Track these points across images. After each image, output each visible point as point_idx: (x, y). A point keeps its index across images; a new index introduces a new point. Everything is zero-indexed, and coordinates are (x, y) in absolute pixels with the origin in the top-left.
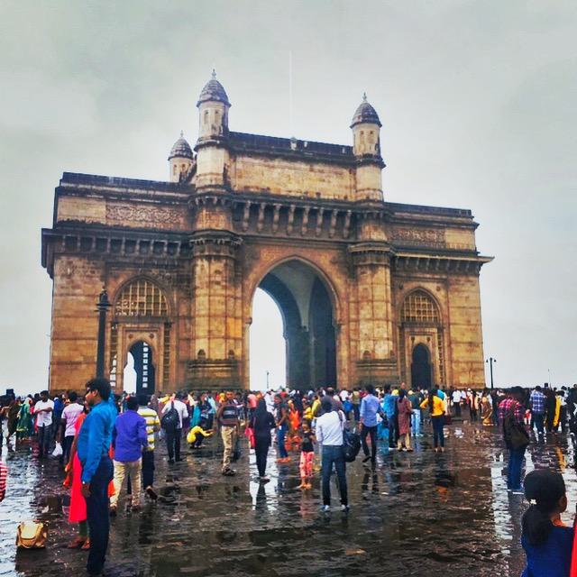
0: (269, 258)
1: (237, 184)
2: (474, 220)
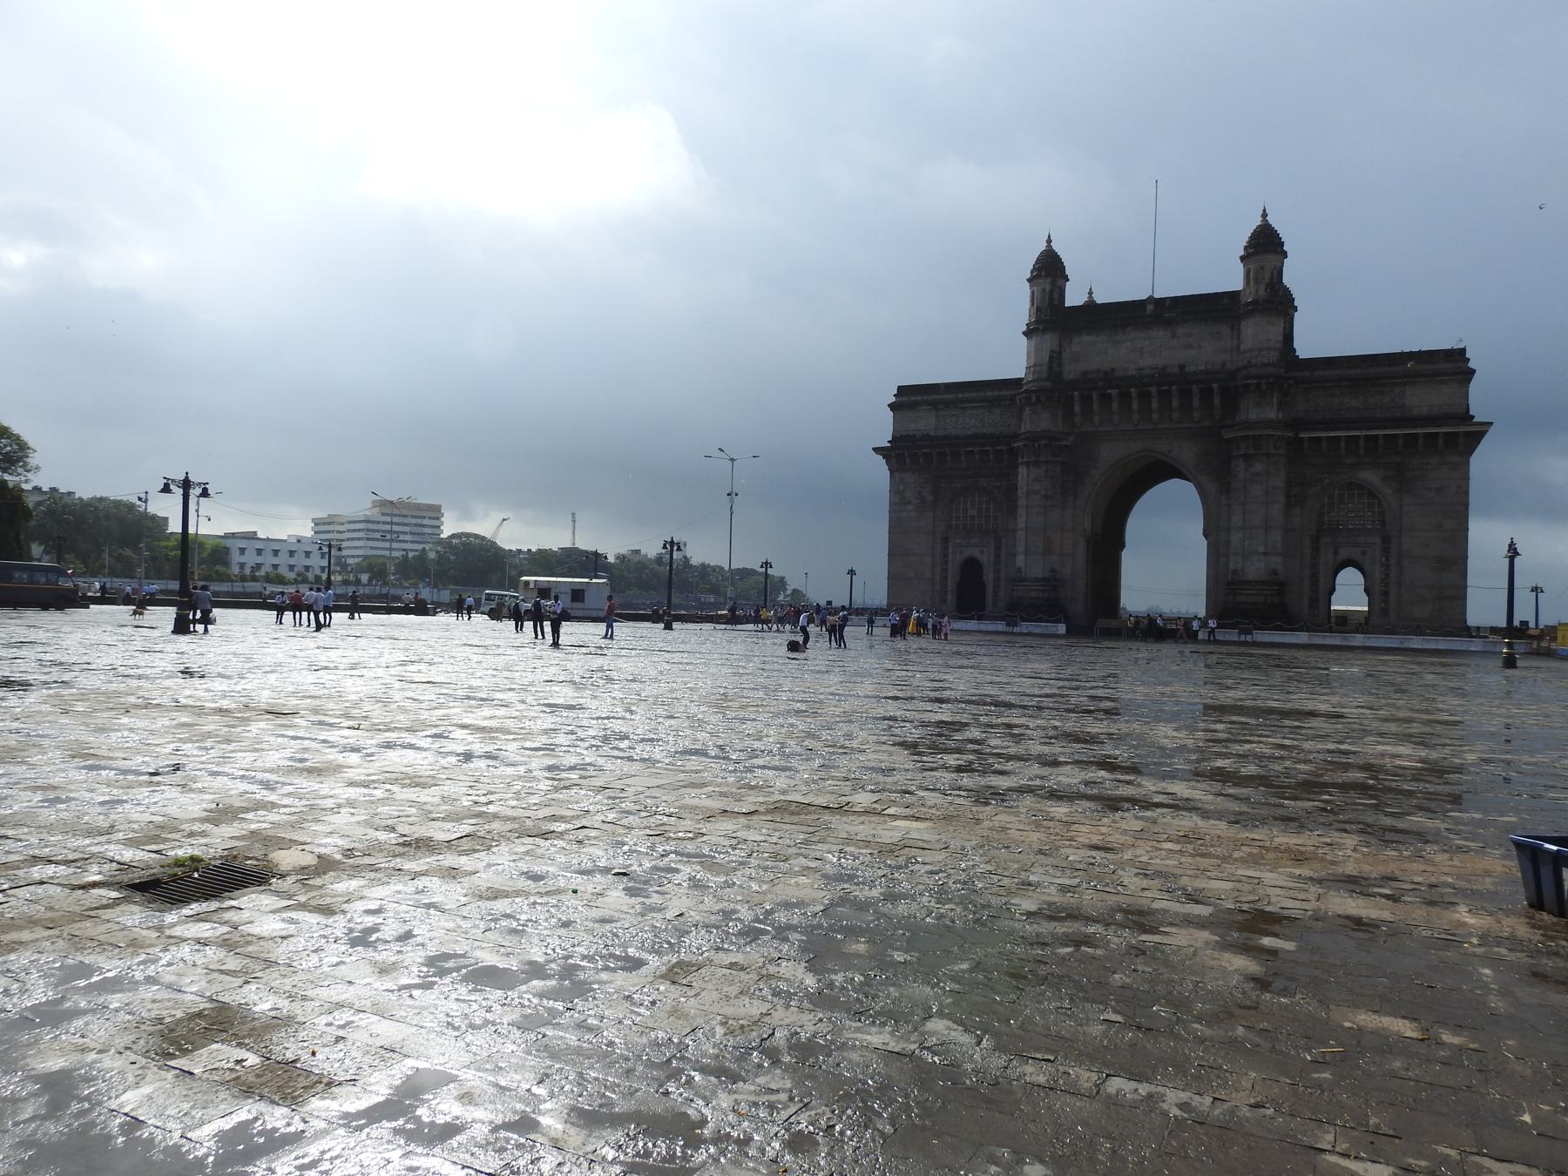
0: (1112, 453)
1: (1071, 371)
2: (1471, 365)
